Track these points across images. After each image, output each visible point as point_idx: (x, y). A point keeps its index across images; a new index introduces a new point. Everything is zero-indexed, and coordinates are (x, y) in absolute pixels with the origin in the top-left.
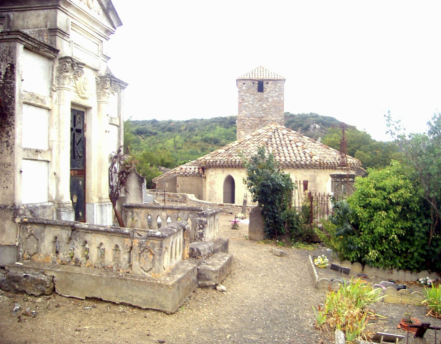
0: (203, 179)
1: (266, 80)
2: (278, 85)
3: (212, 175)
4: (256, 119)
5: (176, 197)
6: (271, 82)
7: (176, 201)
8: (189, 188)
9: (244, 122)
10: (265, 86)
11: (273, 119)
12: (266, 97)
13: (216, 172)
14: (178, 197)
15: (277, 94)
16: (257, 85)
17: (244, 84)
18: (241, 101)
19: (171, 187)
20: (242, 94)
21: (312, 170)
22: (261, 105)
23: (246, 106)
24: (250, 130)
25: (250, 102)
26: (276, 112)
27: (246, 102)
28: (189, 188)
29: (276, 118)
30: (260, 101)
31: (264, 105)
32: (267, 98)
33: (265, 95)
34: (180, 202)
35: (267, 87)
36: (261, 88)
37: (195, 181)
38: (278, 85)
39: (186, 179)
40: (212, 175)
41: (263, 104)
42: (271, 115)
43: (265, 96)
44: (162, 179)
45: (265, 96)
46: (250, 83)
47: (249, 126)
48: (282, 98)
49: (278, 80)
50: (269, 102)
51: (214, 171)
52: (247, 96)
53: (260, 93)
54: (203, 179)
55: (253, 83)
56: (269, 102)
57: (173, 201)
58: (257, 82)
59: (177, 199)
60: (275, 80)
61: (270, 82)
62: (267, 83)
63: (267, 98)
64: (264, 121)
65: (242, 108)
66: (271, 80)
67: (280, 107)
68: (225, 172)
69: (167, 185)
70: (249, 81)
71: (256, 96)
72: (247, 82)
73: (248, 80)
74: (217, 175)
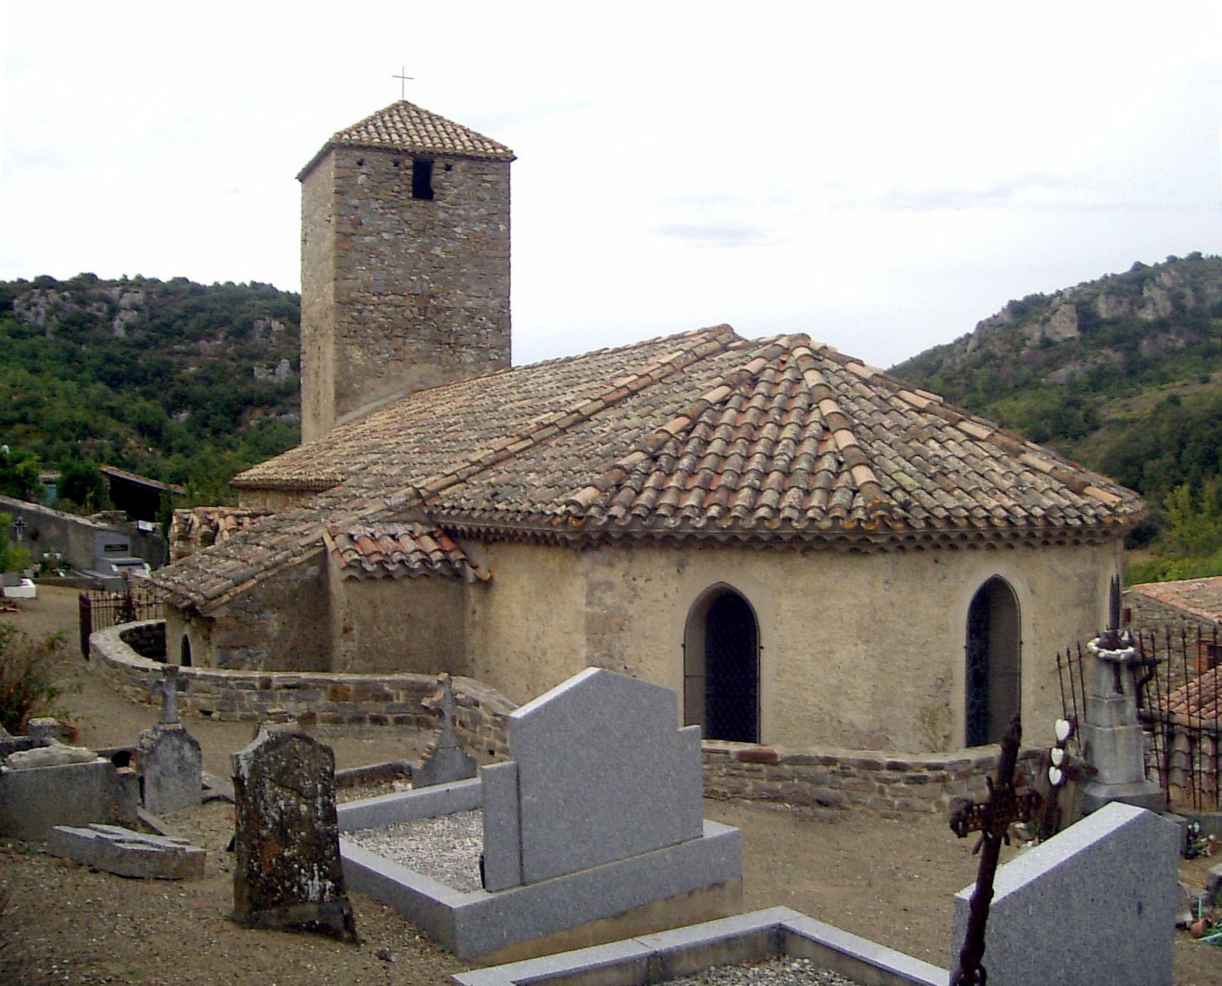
0: (473, 593)
1: (446, 155)
2: (489, 178)
3: (610, 586)
4: (407, 302)
5: (377, 698)
6: (464, 164)
7: (378, 720)
8: (402, 638)
9: (360, 312)
10: (438, 176)
11: (470, 303)
12: (445, 221)
13: (635, 572)
14: (388, 697)
15: (483, 211)
16: (410, 172)
17: (360, 164)
18: (349, 229)
19: (293, 635)
20: (355, 202)
21: (1085, 552)
22: (424, 249)
23: (371, 250)
24: (385, 342)
25: (385, 235)
26: (480, 278)
27: (370, 234)
28: (402, 638)
29: (482, 301)
30: (421, 232)
31: (437, 250)
32: (447, 225)
33: (439, 211)
34: (399, 721)
35: (450, 184)
36: (423, 188)
37: (429, 602)
38: (489, 178)
39: (389, 590)
40: (610, 586)
41: (432, 245)
42: (465, 288)
43: (441, 215)
44: (249, 593)
45: (441, 215)
46: (384, 163)
47: (381, 327)
48: (502, 227)
49: (488, 158)
50: (455, 239)
51: (622, 566)
52: (372, 213)
53: (421, 203)
54: (473, 593)
55: (396, 165)
56: (455, 239)
57: (359, 720)
58: (409, 163)
59: (373, 708)
60: (480, 159)
61: (460, 166)
62: (448, 168)
63: (447, 225)
64: (439, 311)
65: (354, 255)
66: (463, 157)
67: (497, 261)
68: (690, 570)
69: (273, 623)
70: (381, 156)
71: (408, 215)
72: (369, 156)
73: (378, 149)
74: (641, 582)
